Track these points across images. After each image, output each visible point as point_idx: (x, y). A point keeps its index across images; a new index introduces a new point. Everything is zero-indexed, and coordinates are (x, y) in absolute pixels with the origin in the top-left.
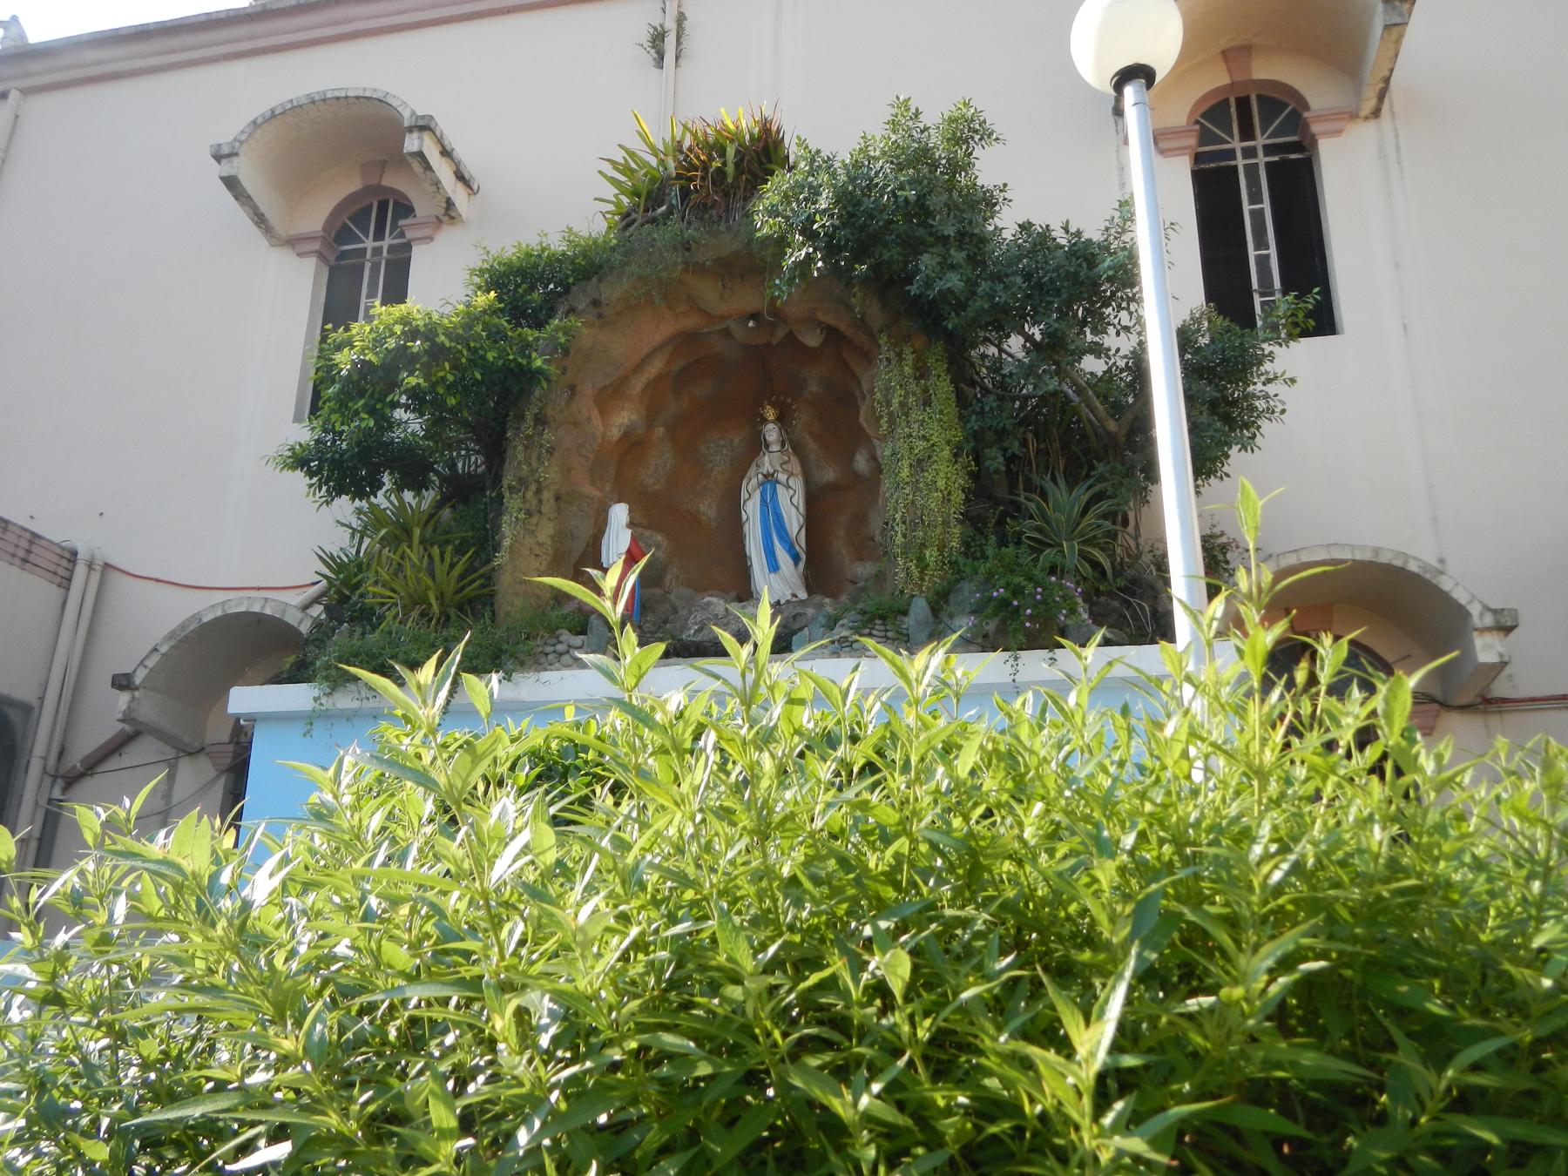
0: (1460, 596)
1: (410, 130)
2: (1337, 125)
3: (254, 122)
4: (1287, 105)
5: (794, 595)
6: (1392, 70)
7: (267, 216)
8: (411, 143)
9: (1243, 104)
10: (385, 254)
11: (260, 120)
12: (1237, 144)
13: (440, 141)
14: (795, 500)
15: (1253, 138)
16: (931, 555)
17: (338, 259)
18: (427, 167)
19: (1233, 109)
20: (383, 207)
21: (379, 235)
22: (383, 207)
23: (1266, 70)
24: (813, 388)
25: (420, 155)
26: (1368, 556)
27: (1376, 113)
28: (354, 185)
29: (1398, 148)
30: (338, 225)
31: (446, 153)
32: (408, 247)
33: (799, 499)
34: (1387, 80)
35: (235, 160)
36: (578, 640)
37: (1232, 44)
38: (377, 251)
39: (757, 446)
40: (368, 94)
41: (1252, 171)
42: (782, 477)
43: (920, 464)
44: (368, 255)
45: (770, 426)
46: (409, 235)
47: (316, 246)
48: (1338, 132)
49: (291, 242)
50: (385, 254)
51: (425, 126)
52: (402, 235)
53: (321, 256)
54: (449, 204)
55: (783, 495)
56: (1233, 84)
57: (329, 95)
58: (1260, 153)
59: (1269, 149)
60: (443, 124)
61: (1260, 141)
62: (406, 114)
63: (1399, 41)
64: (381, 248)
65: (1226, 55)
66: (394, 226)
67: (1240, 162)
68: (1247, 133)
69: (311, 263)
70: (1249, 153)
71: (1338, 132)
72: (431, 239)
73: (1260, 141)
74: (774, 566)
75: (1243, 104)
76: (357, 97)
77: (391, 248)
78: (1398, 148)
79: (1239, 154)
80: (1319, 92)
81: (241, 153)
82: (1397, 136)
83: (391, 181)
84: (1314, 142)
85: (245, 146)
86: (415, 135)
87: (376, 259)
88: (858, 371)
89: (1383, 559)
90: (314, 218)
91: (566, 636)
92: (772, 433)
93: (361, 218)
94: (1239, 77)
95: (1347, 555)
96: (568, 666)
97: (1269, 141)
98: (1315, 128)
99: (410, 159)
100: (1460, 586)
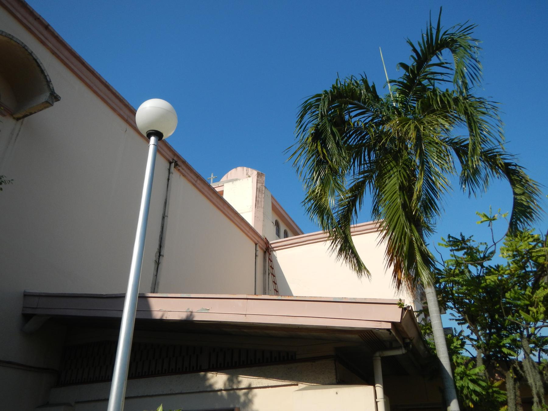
6: (35, 113)
27: (18, 119)
29: (18, 134)
34: (31, 114)
63: (45, 108)
78: (18, 134)
82: (19, 131)
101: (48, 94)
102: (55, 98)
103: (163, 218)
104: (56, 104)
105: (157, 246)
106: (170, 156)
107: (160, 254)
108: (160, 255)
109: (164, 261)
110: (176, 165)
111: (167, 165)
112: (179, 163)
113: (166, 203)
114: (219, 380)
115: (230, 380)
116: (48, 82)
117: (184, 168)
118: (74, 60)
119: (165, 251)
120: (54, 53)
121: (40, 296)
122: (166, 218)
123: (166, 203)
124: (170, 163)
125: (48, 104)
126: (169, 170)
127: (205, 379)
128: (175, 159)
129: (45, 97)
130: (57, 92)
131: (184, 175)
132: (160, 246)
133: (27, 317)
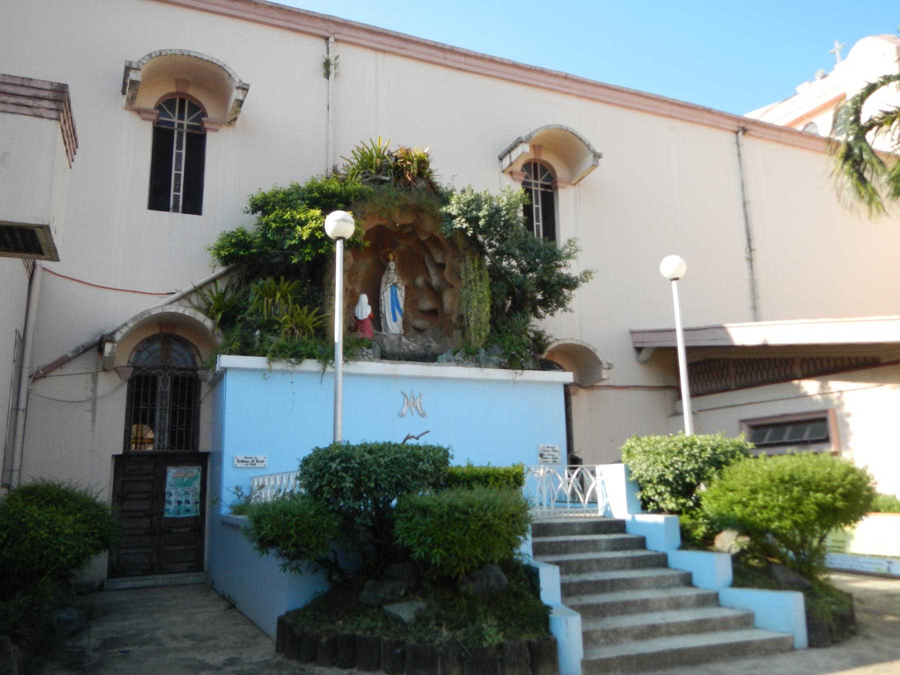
0: (601, 358)
1: (238, 88)
3: (150, 55)
10: (185, 128)
11: (153, 55)
16: (483, 334)
20: (182, 102)
21: (181, 117)
24: (402, 248)
26: (579, 343)
27: (575, 184)
28: (172, 89)
33: (403, 294)
36: (370, 351)
39: (382, 268)
40: (214, 61)
41: (536, 192)
42: (399, 285)
43: (480, 301)
48: (564, 188)
50: (185, 128)
55: (399, 292)
57: (192, 54)
59: (542, 186)
61: (540, 182)
70: (536, 185)
74: (395, 319)
75: (535, 165)
77: (189, 127)
80: (561, 172)
83: (193, 92)
84: (557, 188)
87: (180, 130)
88: (433, 251)
89: (584, 345)
91: (365, 349)
92: (392, 265)
95: (575, 342)
96: (365, 360)
98: (559, 184)
100: (601, 356)
101: (591, 156)
102: (597, 156)
103: (744, 204)
104: (600, 161)
105: (745, 241)
106: (734, 126)
107: (751, 249)
108: (751, 250)
109: (758, 256)
110: (745, 131)
111: (732, 137)
112: (748, 127)
113: (743, 186)
114: (810, 386)
115: (822, 387)
116: (588, 146)
117: (757, 128)
118: (599, 90)
119: (755, 244)
120: (579, 96)
121: (642, 332)
122: (747, 205)
123: (743, 186)
124: (737, 133)
125: (595, 166)
126: (737, 143)
127: (799, 387)
128: (742, 125)
129: (589, 160)
130: (598, 150)
131: (759, 138)
132: (749, 240)
133: (639, 350)
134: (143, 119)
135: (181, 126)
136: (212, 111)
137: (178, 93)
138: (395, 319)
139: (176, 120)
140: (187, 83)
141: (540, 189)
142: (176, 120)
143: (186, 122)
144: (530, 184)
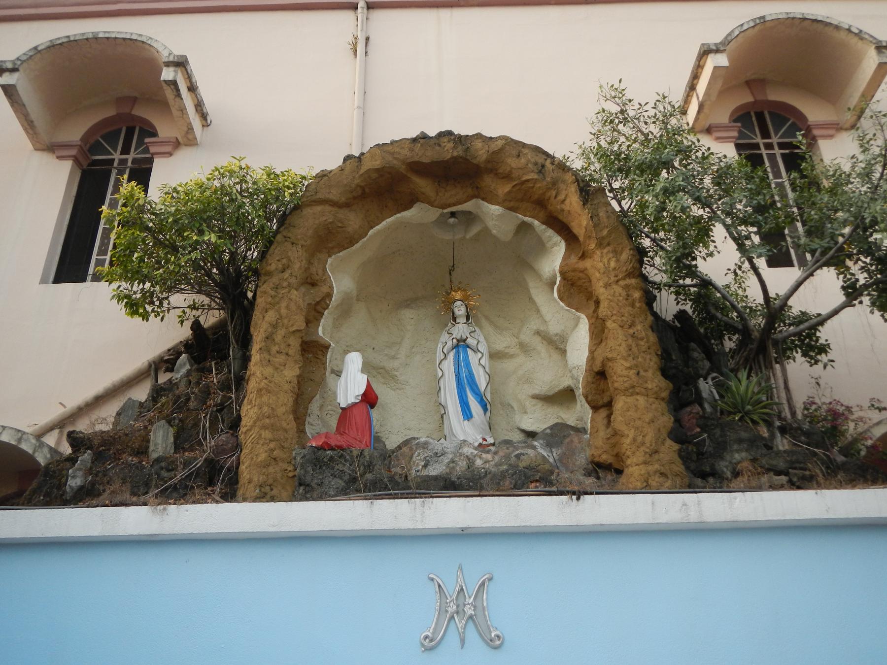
1: (168, 64)
2: (831, 132)
4: (789, 120)
5: (484, 440)
7: (36, 123)
8: (168, 74)
9: (760, 117)
10: (129, 164)
12: (759, 140)
13: (189, 77)
14: (483, 362)
15: (769, 137)
17: (89, 165)
18: (178, 95)
19: (754, 119)
20: (130, 132)
21: (126, 150)
22: (130, 132)
23: (775, 95)
25: (174, 83)
28: (110, 112)
30: (92, 141)
31: (192, 89)
32: (151, 161)
35: (16, 75)
37: (753, 77)
38: (123, 162)
41: (772, 157)
44: (116, 164)
45: (458, 303)
46: (152, 149)
47: (74, 152)
49: (52, 148)
50: (129, 164)
51: (181, 64)
52: (147, 150)
53: (76, 160)
54: (190, 129)
56: (755, 103)
57: (101, 35)
58: (776, 147)
59: (782, 146)
60: (194, 66)
61: (775, 140)
62: (165, 53)
64: (126, 160)
65: (748, 83)
66: (140, 143)
67: (764, 152)
68: (765, 134)
69: (67, 166)
70: (769, 146)
71: (831, 136)
72: (170, 154)
73: (775, 140)
76: (124, 39)
77: (135, 161)
79: (762, 147)
80: (815, 113)
81: (20, 69)
83: (140, 112)
85: (25, 65)
86: (172, 69)
90: (75, 132)
93: (112, 138)
94: (760, 97)
97: (781, 140)
98: (816, 132)
99: (165, 86)
116: (860, 35)
134: (60, 158)
135: (123, 162)
136: (165, 130)
137: (118, 118)
138: (467, 414)
139: (117, 156)
140: (134, 100)
141: (778, 152)
142: (117, 156)
143: (130, 158)
144: (756, 146)
